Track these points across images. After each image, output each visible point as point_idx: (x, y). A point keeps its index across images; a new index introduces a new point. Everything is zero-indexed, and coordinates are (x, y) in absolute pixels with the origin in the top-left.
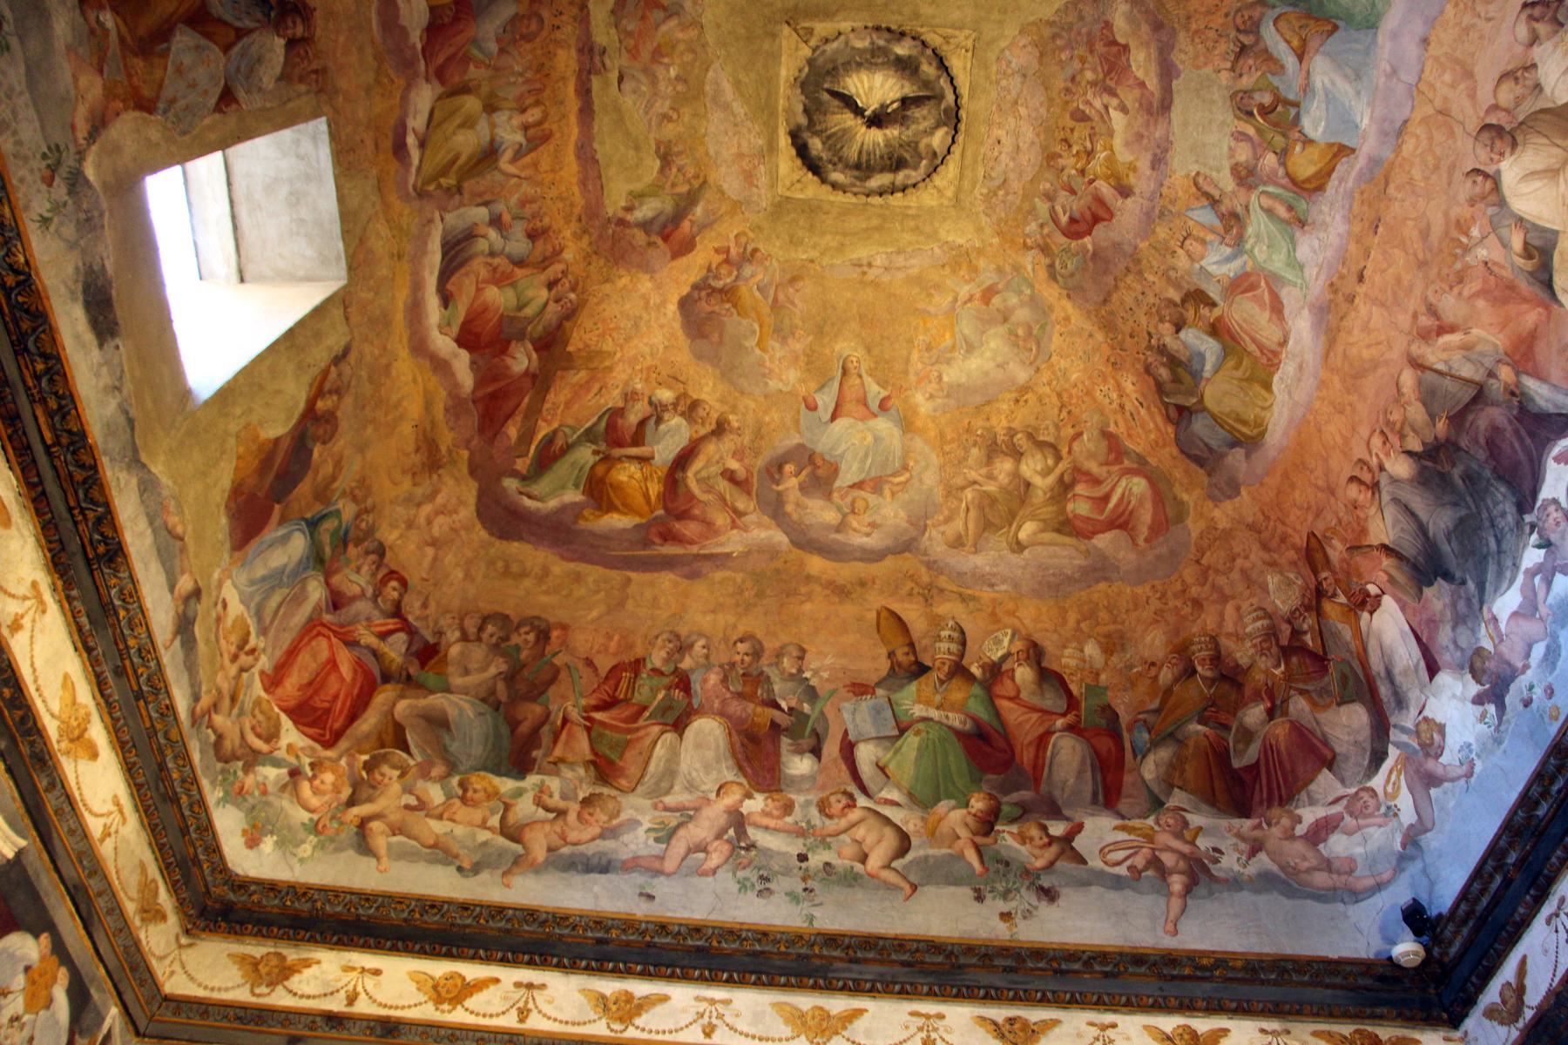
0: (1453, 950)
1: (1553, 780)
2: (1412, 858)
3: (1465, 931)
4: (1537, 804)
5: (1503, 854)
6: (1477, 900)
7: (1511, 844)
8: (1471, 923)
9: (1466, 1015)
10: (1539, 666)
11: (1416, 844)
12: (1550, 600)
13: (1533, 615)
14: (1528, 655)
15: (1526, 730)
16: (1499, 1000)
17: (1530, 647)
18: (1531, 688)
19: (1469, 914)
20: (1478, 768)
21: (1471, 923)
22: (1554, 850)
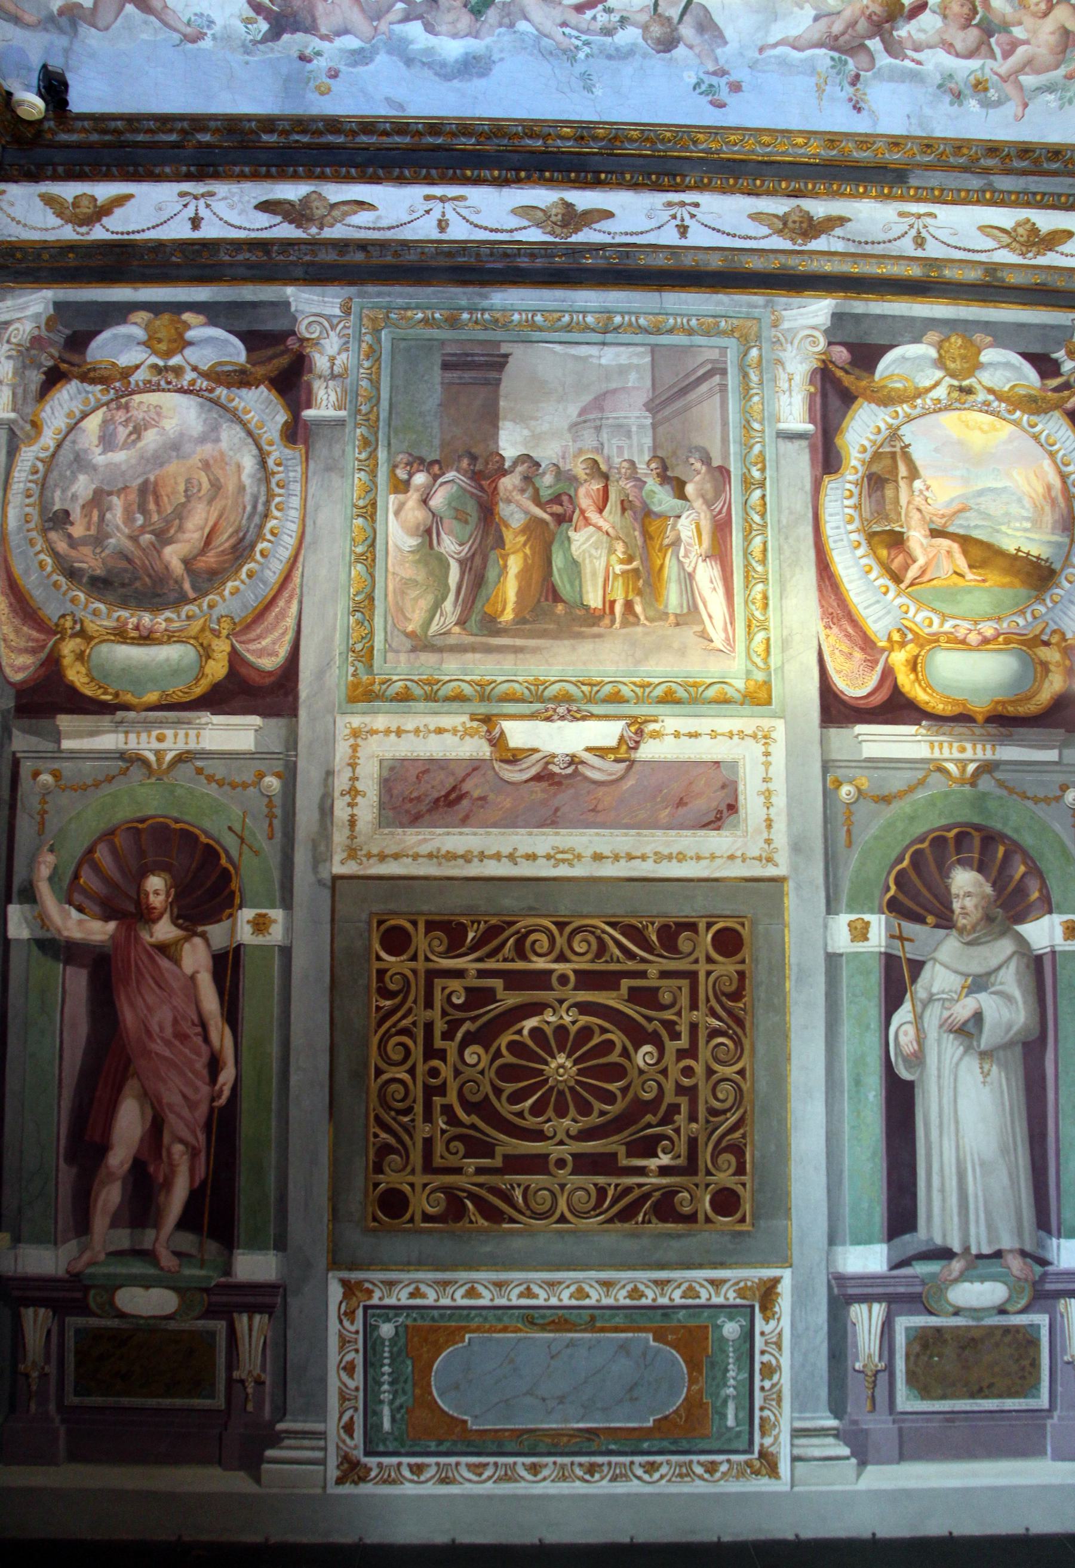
0: (64, 137)
1: (304, 132)
2: (61, 30)
3: (95, 137)
4: (271, 131)
5: (204, 129)
6: (136, 131)
7: (217, 131)
8: (107, 138)
9: (16, 182)
10: (341, 50)
11: (74, 25)
12: (397, 28)
13: (372, 19)
14: (339, 34)
15: (284, 70)
16: (70, 200)
17: (346, 32)
18: (319, 54)
19: (116, 132)
20: (206, 44)
21: (107, 138)
22: (245, 164)
